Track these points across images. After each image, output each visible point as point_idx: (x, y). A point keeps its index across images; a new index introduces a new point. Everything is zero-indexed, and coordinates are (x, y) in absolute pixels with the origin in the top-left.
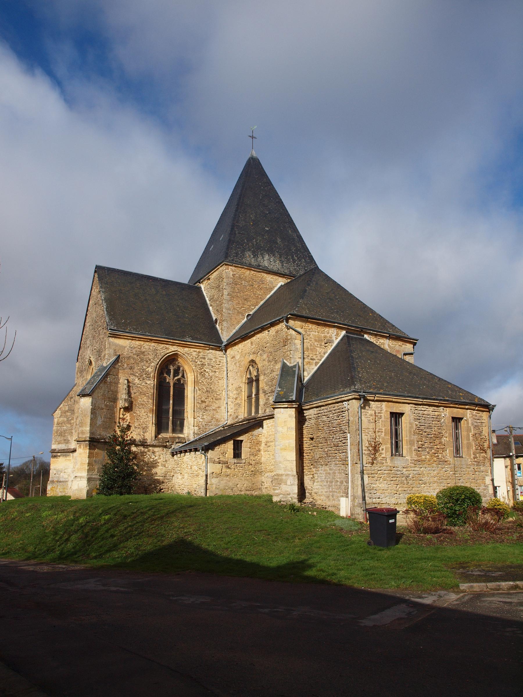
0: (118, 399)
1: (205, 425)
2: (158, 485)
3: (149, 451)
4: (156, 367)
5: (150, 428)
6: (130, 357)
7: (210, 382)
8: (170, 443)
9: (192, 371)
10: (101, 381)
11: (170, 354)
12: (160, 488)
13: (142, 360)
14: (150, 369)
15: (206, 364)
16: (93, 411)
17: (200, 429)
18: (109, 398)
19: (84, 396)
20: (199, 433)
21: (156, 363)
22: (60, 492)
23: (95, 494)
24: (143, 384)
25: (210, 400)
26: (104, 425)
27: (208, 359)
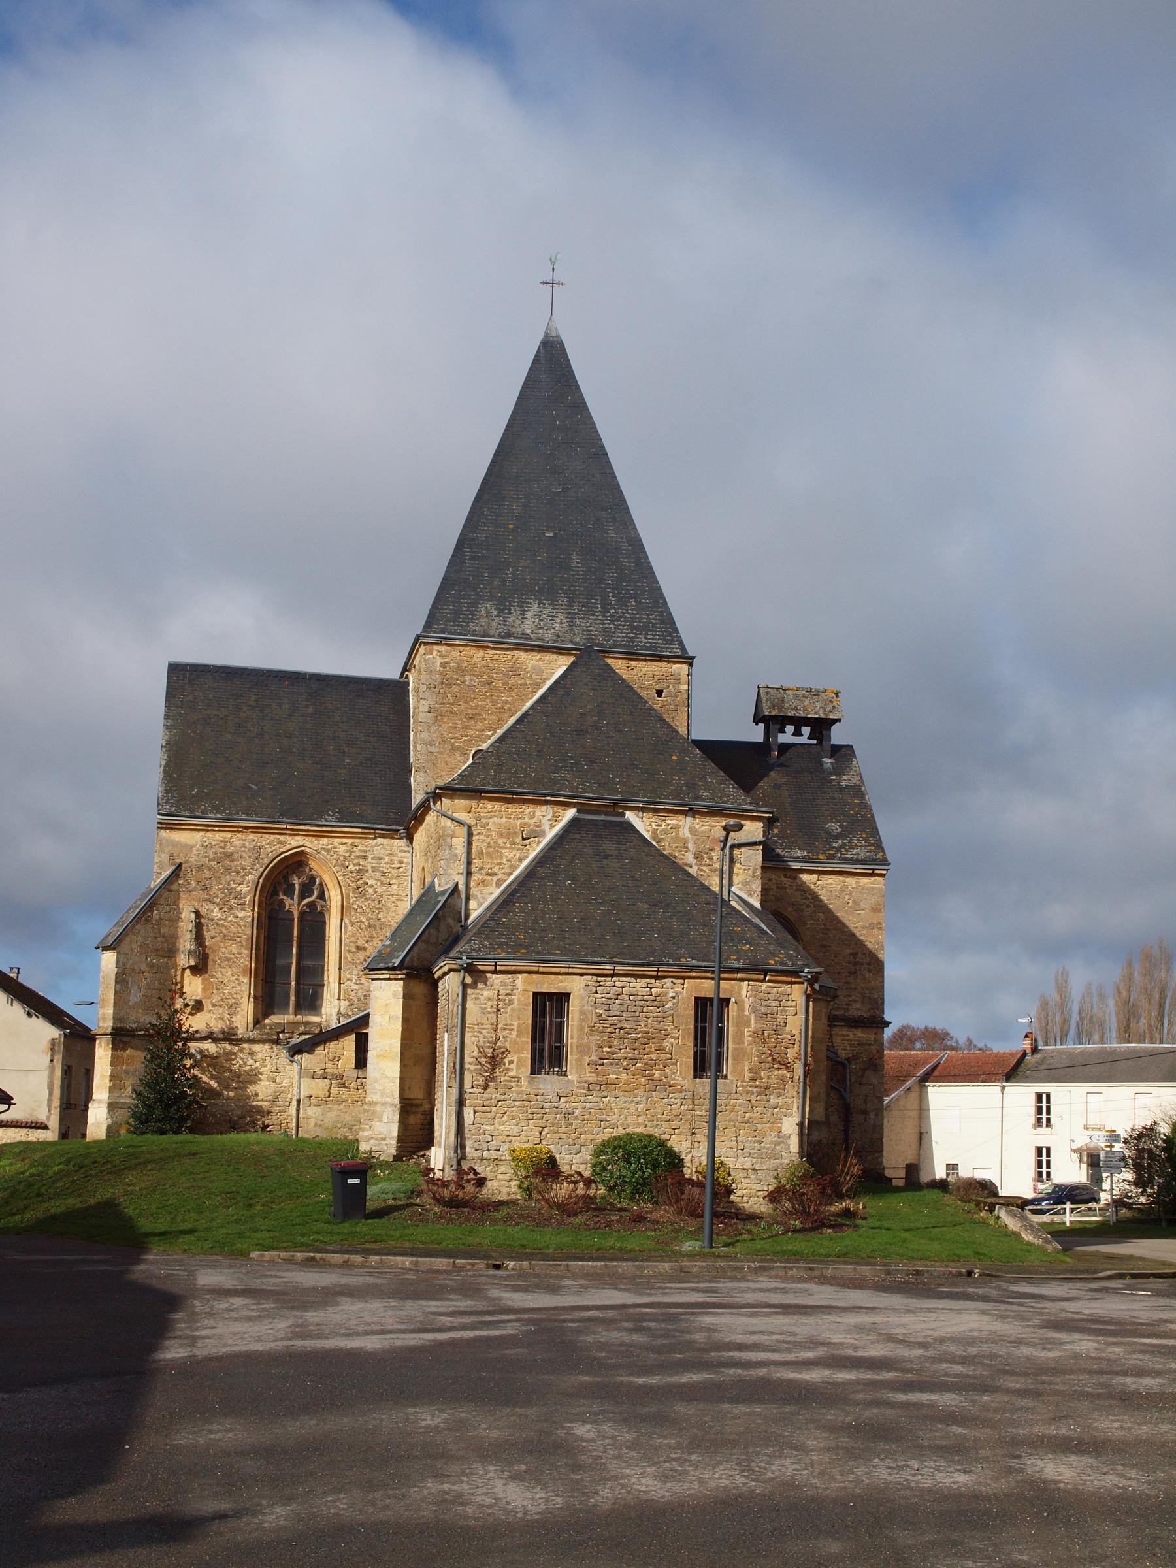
0: (178, 950)
1: (365, 996)
2: (259, 1117)
3: (241, 1050)
4: (259, 882)
5: (244, 1006)
6: (202, 865)
7: (377, 906)
8: (287, 1035)
9: (337, 885)
10: (137, 919)
11: (286, 854)
12: (263, 1123)
13: (228, 871)
14: (244, 888)
15: (370, 868)
16: (121, 978)
17: (352, 1005)
18: (157, 950)
19: (106, 949)
20: (350, 1013)
21: (258, 875)
23: (125, 1131)
24: (229, 919)
25: (375, 945)
26: (145, 1002)
27: (373, 859)
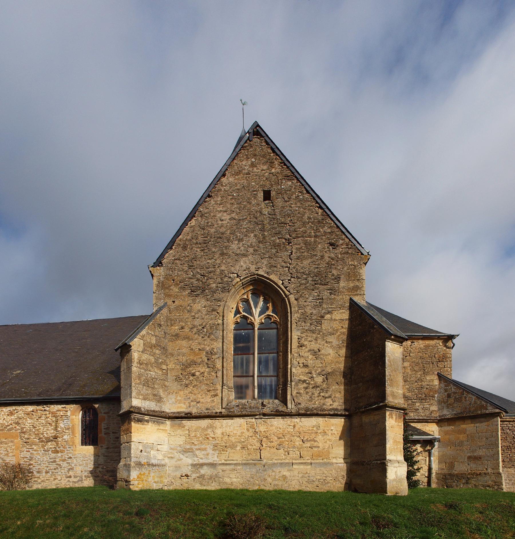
22: (155, 482)
